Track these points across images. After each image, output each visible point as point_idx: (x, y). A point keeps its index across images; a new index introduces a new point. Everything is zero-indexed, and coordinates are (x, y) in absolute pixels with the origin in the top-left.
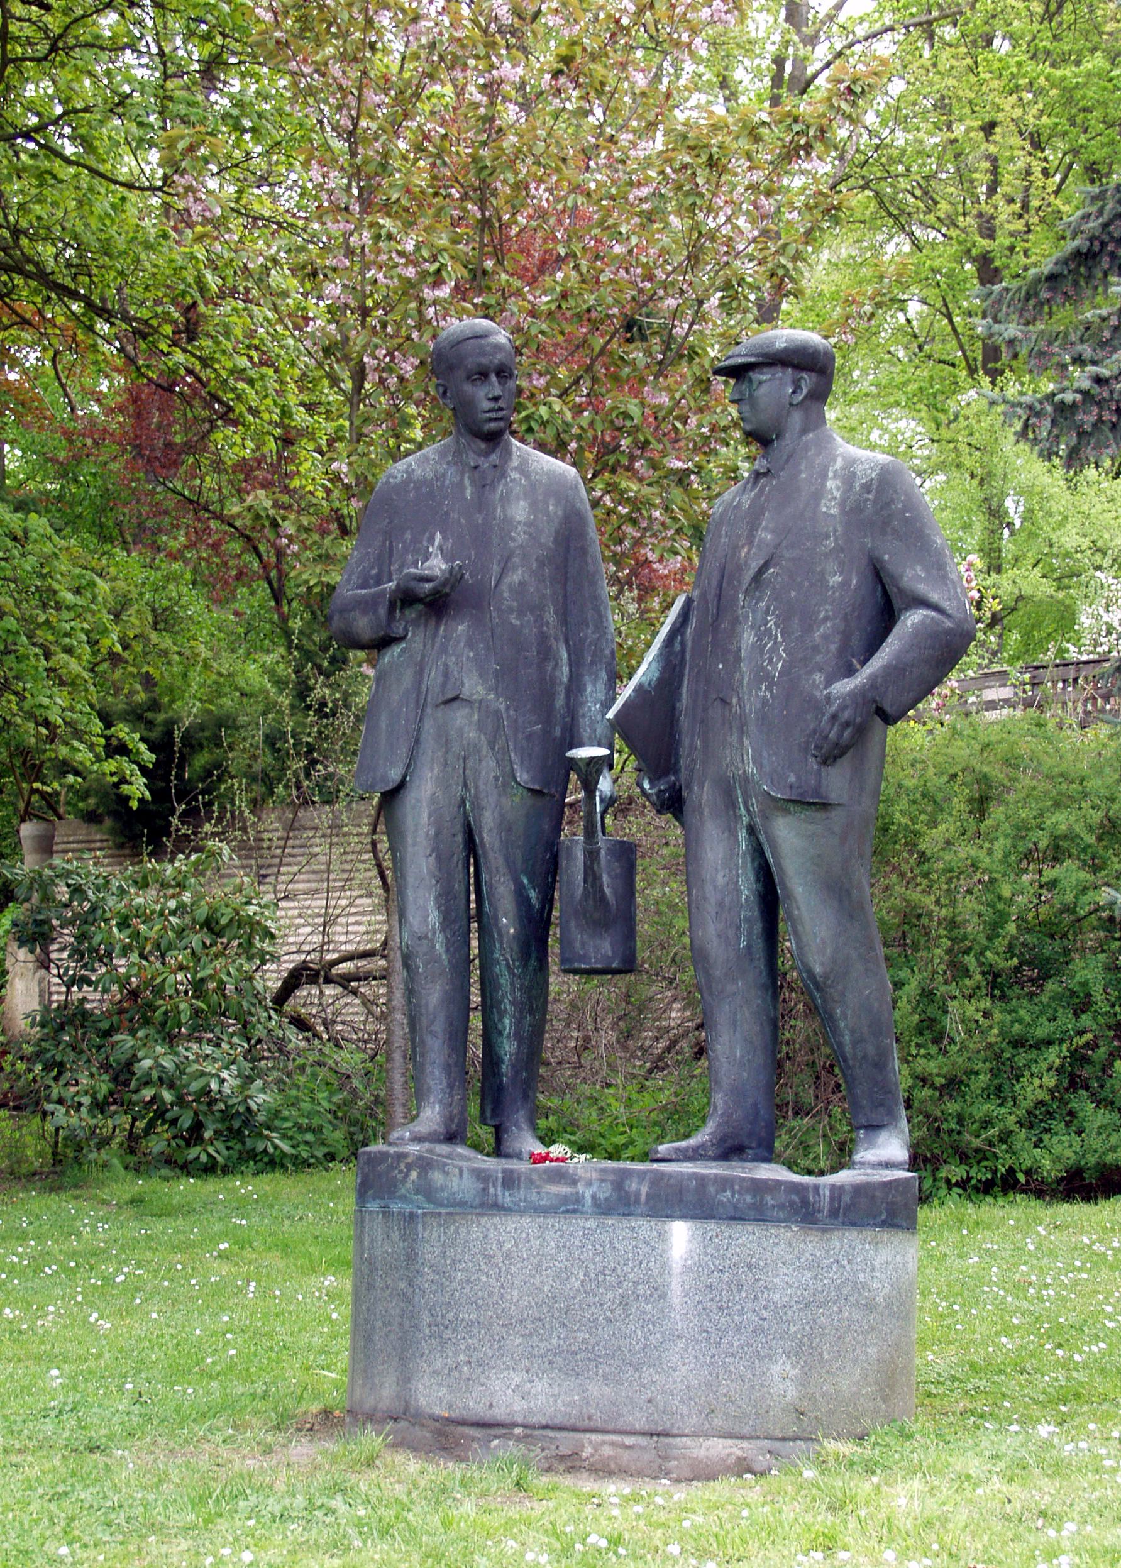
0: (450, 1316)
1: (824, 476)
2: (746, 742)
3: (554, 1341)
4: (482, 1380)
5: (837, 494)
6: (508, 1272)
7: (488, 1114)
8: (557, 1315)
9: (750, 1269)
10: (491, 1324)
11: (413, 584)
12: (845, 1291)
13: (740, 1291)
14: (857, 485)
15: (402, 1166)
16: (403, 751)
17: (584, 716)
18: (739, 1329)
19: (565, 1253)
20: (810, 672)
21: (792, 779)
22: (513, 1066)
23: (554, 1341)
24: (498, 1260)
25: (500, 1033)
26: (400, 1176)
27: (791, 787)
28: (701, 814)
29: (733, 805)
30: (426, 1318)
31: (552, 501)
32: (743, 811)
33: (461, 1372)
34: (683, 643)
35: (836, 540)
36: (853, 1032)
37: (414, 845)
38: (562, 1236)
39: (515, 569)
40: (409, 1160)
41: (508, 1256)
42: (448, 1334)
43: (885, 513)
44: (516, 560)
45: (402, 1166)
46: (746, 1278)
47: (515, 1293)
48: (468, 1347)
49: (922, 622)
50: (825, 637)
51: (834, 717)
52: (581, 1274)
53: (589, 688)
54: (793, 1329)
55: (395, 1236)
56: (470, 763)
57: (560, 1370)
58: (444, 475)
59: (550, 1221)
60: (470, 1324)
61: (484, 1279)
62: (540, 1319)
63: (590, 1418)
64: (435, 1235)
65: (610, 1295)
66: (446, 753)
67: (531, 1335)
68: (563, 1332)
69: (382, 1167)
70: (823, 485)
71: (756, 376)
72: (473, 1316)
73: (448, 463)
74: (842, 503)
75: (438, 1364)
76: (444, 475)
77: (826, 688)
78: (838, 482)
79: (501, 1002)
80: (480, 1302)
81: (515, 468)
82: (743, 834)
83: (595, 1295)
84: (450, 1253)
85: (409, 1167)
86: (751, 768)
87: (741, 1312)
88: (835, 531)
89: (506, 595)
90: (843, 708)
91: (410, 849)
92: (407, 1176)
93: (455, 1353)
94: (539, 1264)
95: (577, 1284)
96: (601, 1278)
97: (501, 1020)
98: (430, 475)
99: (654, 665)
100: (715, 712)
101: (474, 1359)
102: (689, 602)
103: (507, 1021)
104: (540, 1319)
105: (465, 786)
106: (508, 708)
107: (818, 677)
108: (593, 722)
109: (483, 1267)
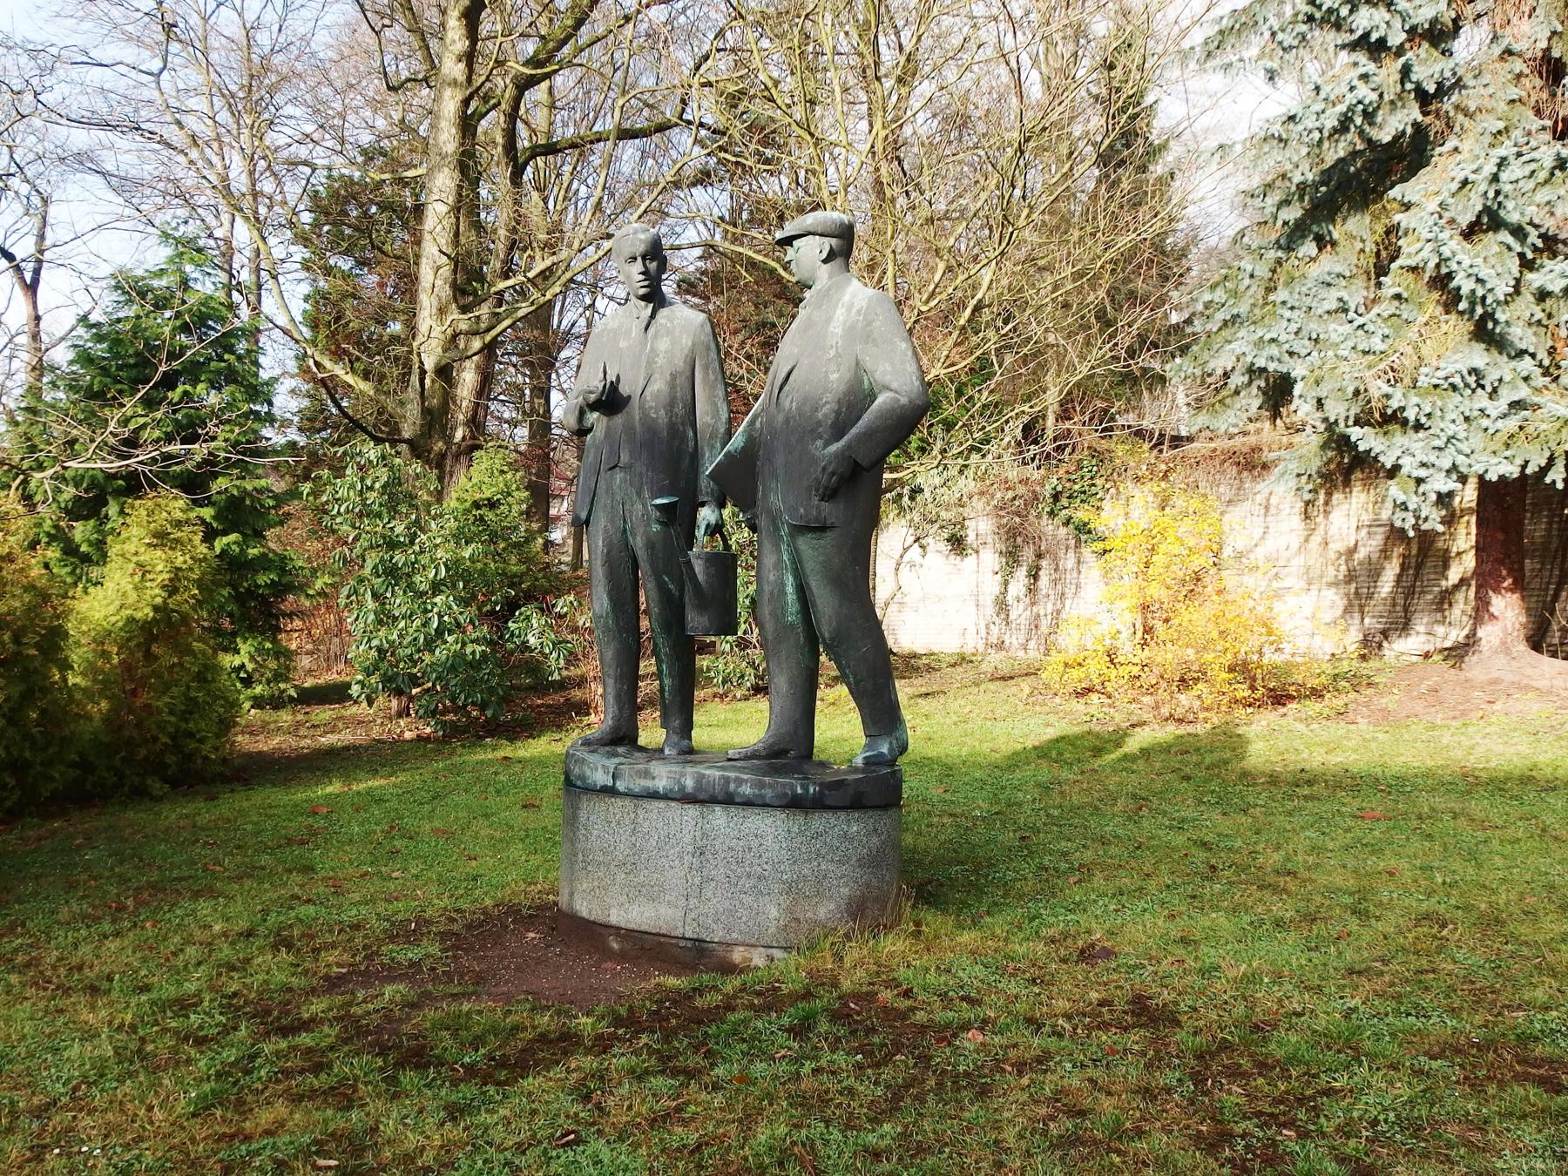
12: (823, 851)
18: (749, 875)
20: (814, 440)
46: (754, 843)
50: (825, 415)
51: (824, 469)
82: (784, 547)
107: (819, 443)
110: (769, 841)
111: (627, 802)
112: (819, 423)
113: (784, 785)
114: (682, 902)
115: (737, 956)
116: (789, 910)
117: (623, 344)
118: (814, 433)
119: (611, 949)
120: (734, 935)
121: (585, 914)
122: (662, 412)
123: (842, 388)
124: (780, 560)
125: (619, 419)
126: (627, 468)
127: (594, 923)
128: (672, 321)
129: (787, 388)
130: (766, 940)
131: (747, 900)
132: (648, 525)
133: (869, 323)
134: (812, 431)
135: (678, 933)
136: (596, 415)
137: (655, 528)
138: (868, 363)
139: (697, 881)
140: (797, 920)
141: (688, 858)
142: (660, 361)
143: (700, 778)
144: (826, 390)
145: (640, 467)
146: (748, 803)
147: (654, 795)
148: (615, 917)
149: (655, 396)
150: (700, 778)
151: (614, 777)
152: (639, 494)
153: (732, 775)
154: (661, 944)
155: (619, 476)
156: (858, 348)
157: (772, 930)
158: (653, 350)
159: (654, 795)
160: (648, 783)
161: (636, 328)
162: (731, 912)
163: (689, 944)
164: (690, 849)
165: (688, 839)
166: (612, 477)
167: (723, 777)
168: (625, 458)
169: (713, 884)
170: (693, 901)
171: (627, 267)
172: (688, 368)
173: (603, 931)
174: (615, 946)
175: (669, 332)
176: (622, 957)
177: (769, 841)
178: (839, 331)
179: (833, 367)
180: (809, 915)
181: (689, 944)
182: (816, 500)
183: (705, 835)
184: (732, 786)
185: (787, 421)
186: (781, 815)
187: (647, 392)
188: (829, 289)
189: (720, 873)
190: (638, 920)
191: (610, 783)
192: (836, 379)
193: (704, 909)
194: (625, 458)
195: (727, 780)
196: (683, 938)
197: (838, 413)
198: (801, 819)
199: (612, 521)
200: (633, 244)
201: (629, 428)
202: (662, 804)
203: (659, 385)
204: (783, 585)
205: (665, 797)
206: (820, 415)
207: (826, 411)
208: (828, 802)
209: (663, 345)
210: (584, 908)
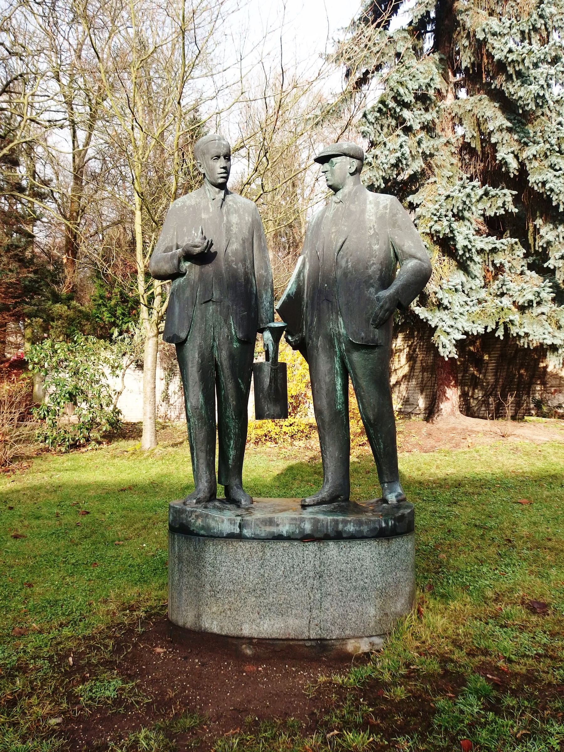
0: (220, 587)
1: (365, 204)
2: (340, 319)
3: (271, 599)
4: (237, 617)
5: (372, 211)
6: (247, 567)
7: (223, 480)
8: (271, 587)
9: (359, 560)
10: (240, 591)
12: (398, 564)
13: (355, 571)
14: (381, 207)
15: (194, 516)
16: (186, 324)
18: (355, 588)
19: (275, 558)
20: (368, 288)
21: (363, 334)
23: (271, 599)
24: (243, 561)
26: (193, 521)
29: (334, 347)
30: (208, 587)
31: (246, 215)
32: (337, 349)
33: (226, 614)
34: (303, 276)
35: (374, 230)
36: (384, 443)
37: (192, 367)
38: (273, 551)
39: (233, 243)
40: (197, 514)
42: (218, 596)
43: (394, 218)
45: (194, 516)
46: (358, 565)
47: (251, 577)
48: (229, 602)
49: (415, 265)
50: (374, 272)
51: (382, 307)
53: (264, 297)
54: (378, 586)
56: (217, 330)
57: (274, 613)
58: (199, 203)
59: (268, 544)
60: (230, 591)
61: (236, 570)
62: (264, 589)
63: (289, 634)
64: (211, 549)
65: (296, 577)
67: (259, 597)
68: (275, 595)
69: (184, 516)
70: (366, 207)
71: (334, 160)
72: (231, 588)
74: (376, 213)
75: (214, 609)
76: (199, 203)
77: (376, 294)
78: (373, 206)
80: (234, 581)
82: (337, 359)
83: (289, 578)
84: (219, 558)
85: (197, 517)
86: (343, 331)
88: (374, 226)
90: (386, 303)
91: (190, 369)
92: (196, 521)
93: (223, 604)
94: (262, 564)
95: (281, 573)
96: (292, 569)
97: (229, 441)
98: (193, 203)
99: (294, 285)
100: (324, 306)
101: (232, 608)
102: (304, 259)
105: (214, 340)
106: (232, 305)
107: (372, 290)
108: (267, 311)
109: (235, 565)
110: (367, 563)
111: (255, 544)
112: (370, 277)
113: (374, 522)
114: (307, 613)
115: (350, 647)
116: (382, 609)
117: (203, 216)
118: (367, 283)
119: (245, 655)
120: (347, 632)
121: (215, 629)
122: (240, 265)
123: (382, 255)
124: (333, 367)
125: (209, 268)
126: (218, 302)
127: (226, 636)
128: (236, 204)
129: (341, 253)
130: (369, 632)
131: (355, 606)
132: (232, 343)
133: (394, 215)
134: (366, 282)
135: (305, 636)
136: (188, 264)
137: (236, 345)
138: (397, 241)
139: (318, 596)
140: (386, 614)
141: (310, 582)
142: (235, 229)
143: (316, 522)
144: (372, 256)
145: (227, 302)
146: (352, 537)
147: (279, 538)
148: (247, 630)
149: (235, 253)
150: (316, 522)
151: (240, 526)
152: (226, 321)
153: (340, 518)
154: (290, 646)
155: (211, 308)
156: (389, 230)
157: (372, 624)
158: (228, 222)
160: (274, 529)
161: (212, 208)
162: (343, 616)
163: (313, 643)
164: (311, 574)
165: (309, 567)
166: (206, 309)
167: (334, 520)
168: (216, 295)
169: (330, 598)
170: (315, 612)
171: (211, 162)
172: (251, 237)
173: (235, 642)
174: (249, 652)
175: (237, 211)
176: (257, 659)
177: (367, 563)
178: (373, 218)
179: (374, 241)
180: (393, 609)
181: (313, 643)
182: (372, 328)
184: (340, 527)
185: (345, 274)
186: (374, 543)
187: (229, 250)
188: (356, 192)
189: (334, 589)
190: (270, 631)
191: (237, 531)
192: (378, 249)
193: (323, 616)
194: (216, 295)
195: (337, 522)
196: (309, 640)
197: (381, 270)
198: (385, 544)
199: (205, 339)
200: (219, 147)
201: (218, 274)
202: (286, 544)
203: (235, 246)
204: (335, 384)
205: (289, 538)
206: (370, 271)
207: (374, 269)
208: (399, 531)
209: (234, 219)
210: (213, 624)
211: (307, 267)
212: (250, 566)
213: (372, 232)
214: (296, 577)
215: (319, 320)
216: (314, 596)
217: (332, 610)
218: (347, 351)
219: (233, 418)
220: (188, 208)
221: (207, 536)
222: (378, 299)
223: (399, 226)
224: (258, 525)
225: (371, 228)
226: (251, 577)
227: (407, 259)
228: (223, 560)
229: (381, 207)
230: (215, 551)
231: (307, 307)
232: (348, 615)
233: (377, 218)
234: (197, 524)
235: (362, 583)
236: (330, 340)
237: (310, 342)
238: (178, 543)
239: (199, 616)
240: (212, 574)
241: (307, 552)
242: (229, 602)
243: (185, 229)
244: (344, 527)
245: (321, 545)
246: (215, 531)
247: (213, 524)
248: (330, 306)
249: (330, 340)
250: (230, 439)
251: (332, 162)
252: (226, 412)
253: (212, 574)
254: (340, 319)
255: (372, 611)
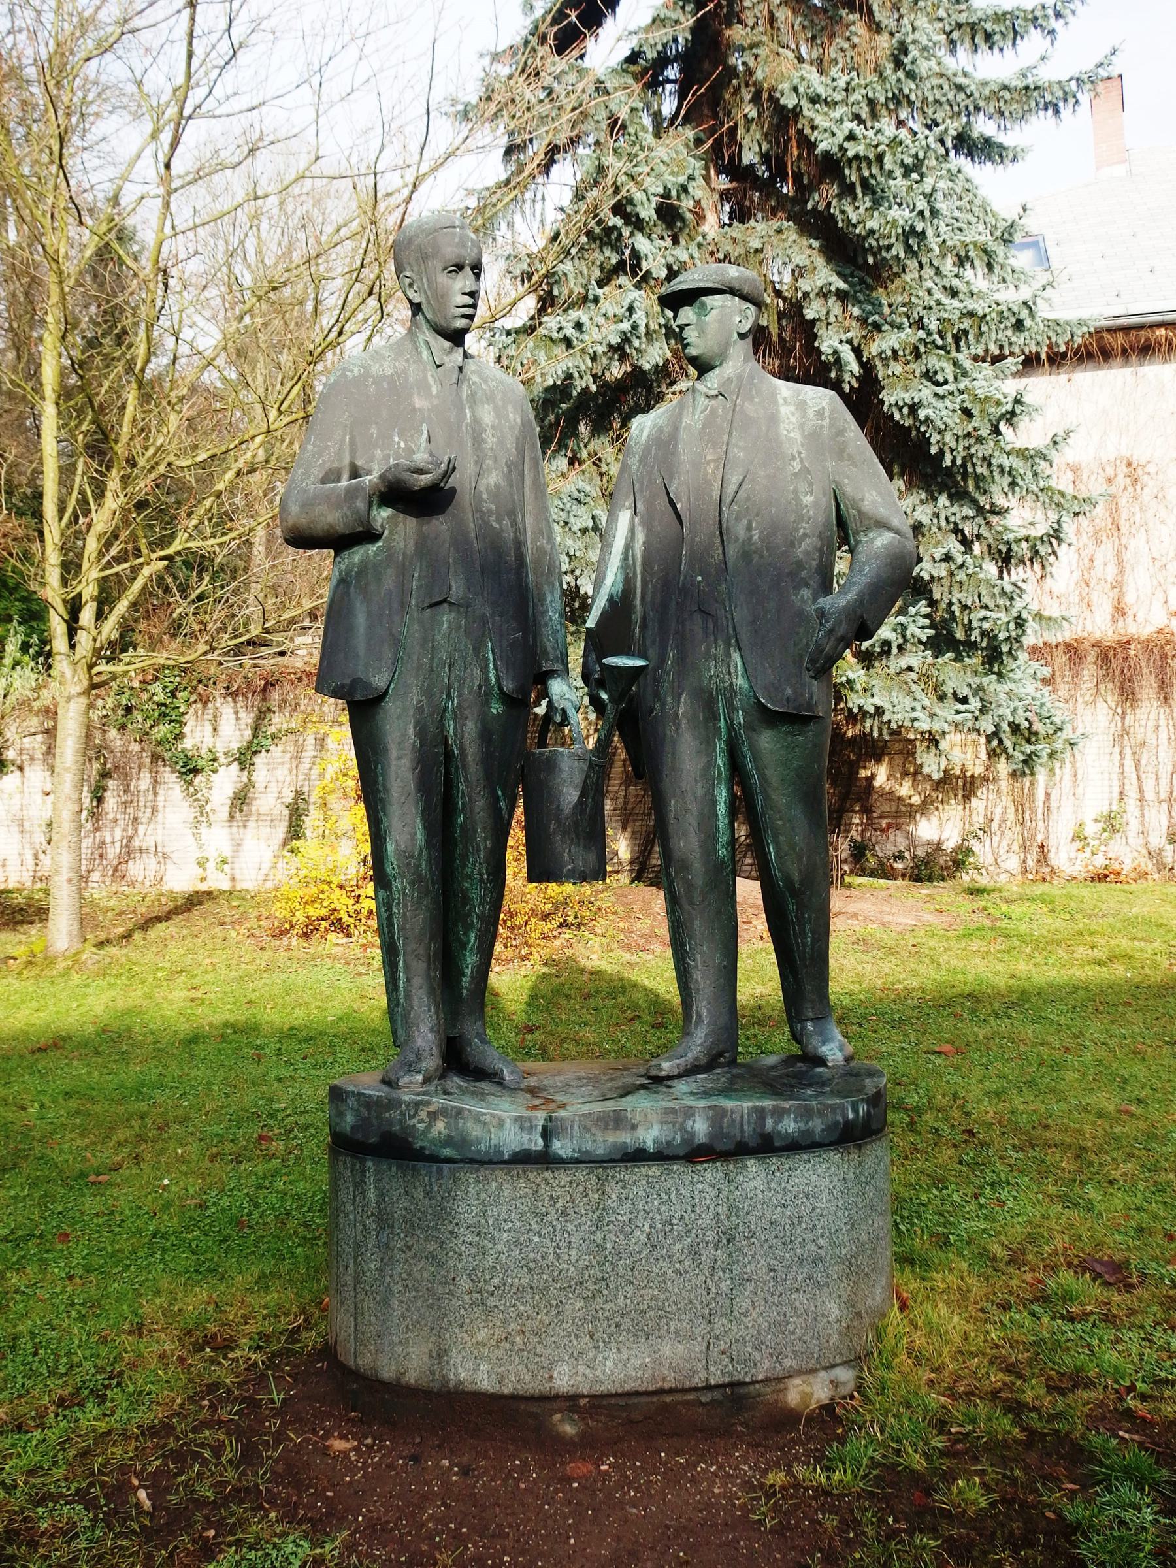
0: (496, 1281)
1: (775, 402)
3: (621, 1301)
4: (539, 1350)
5: (793, 419)
6: (563, 1229)
8: (622, 1272)
9: (807, 1196)
10: (547, 1288)
11: (407, 476)
13: (800, 1223)
14: (811, 412)
16: (388, 655)
17: (546, 625)
18: (801, 1261)
19: (629, 1204)
20: (797, 588)
22: (472, 977)
23: (621, 1301)
25: (464, 946)
26: (421, 1126)
27: (788, 700)
28: (678, 726)
30: (464, 1283)
31: (510, 409)
32: (722, 724)
33: (512, 1343)
36: (813, 933)
37: (399, 758)
38: (624, 1187)
39: (489, 471)
40: (432, 1108)
41: (564, 1213)
42: (491, 1302)
44: (490, 462)
45: (423, 1114)
46: (805, 1210)
47: (573, 1252)
48: (520, 1315)
49: (891, 544)
50: (807, 553)
51: (831, 631)
52: (647, 1228)
55: (419, 1193)
57: (629, 1331)
58: (405, 372)
61: (536, 1239)
62: (603, 1279)
63: (664, 1380)
64: (472, 1192)
65: (678, 1246)
66: (433, 658)
68: (630, 1290)
69: (394, 1115)
70: (778, 411)
71: (708, 300)
72: (525, 1281)
73: (407, 361)
74: (802, 426)
75: (482, 1335)
76: (405, 372)
78: (792, 408)
79: (468, 915)
81: (473, 372)
82: (720, 746)
83: (662, 1248)
84: (492, 1211)
85: (433, 1116)
86: (740, 682)
87: (803, 1245)
89: (485, 496)
90: (839, 622)
91: (394, 762)
92: (429, 1126)
93: (504, 1322)
94: (600, 1219)
95: (643, 1238)
97: (466, 934)
98: (389, 371)
100: (696, 625)
103: (473, 935)
104: (603, 1279)
105: (449, 696)
107: (806, 593)
109: (535, 1226)
110: (823, 1202)
111: (581, 1174)
112: (800, 565)
113: (833, 1109)
114: (701, 1327)
115: (794, 1394)
117: (418, 403)
119: (561, 1439)
120: (787, 1362)
121: (485, 1382)
122: (506, 522)
125: (440, 526)
127: (514, 1397)
128: (485, 381)
130: (830, 1358)
131: (801, 1300)
132: (487, 703)
134: (791, 574)
135: (697, 1381)
136: (386, 513)
137: (496, 708)
139: (725, 1286)
141: (707, 1253)
142: (490, 439)
144: (801, 518)
145: (482, 607)
147: (638, 1156)
148: (564, 1379)
149: (496, 493)
151: (546, 1134)
152: (478, 649)
153: (768, 1103)
154: (666, 1405)
155: (446, 619)
157: (835, 1339)
158: (476, 421)
159: (638, 1156)
160: (625, 1138)
162: (779, 1326)
163: (717, 1395)
164: (710, 1236)
165: (706, 1220)
167: (755, 1110)
168: (457, 589)
169: (750, 1287)
170: (720, 1323)
171: (442, 279)
174: (569, 1429)
175: (490, 399)
176: (589, 1445)
177: (823, 1202)
178: (796, 435)
179: (803, 486)
181: (717, 1395)
183: (733, 1209)
184: (769, 1123)
185: (746, 555)
189: (758, 1268)
190: (619, 1375)
193: (737, 1331)
195: (761, 1113)
196: (709, 1387)
199: (428, 693)
201: (460, 541)
202: (655, 1170)
204: (714, 803)
205: (660, 1156)
206: (800, 551)
209: (487, 416)
210: (478, 1369)
211: (640, 537)
212: (570, 1227)
213: (797, 465)
214: (678, 1246)
215: (681, 659)
216: (717, 1287)
217: (754, 1315)
218: (749, 727)
219: (482, 880)
220: (378, 381)
221: (462, 1161)
222: (822, 614)
223: (850, 457)
224: (587, 1129)
225: (794, 458)
226: (573, 1252)
227: (869, 528)
228: (504, 1216)
229: (811, 412)
230: (483, 1195)
231: (644, 626)
232: (788, 1323)
233: (805, 437)
234: (434, 1132)
235: (814, 1248)
236: (708, 702)
237: (658, 706)
238: (377, 1181)
239: (441, 1354)
240: (474, 1250)
241: (700, 1186)
242: (520, 1315)
243: (374, 431)
244: (777, 1123)
245: (731, 1167)
246: (483, 1147)
247: (474, 1130)
248: (711, 625)
249: (708, 702)
250: (468, 928)
251: (703, 305)
252: (464, 866)
253: (474, 1250)
254: (736, 656)
255: (834, 1310)
